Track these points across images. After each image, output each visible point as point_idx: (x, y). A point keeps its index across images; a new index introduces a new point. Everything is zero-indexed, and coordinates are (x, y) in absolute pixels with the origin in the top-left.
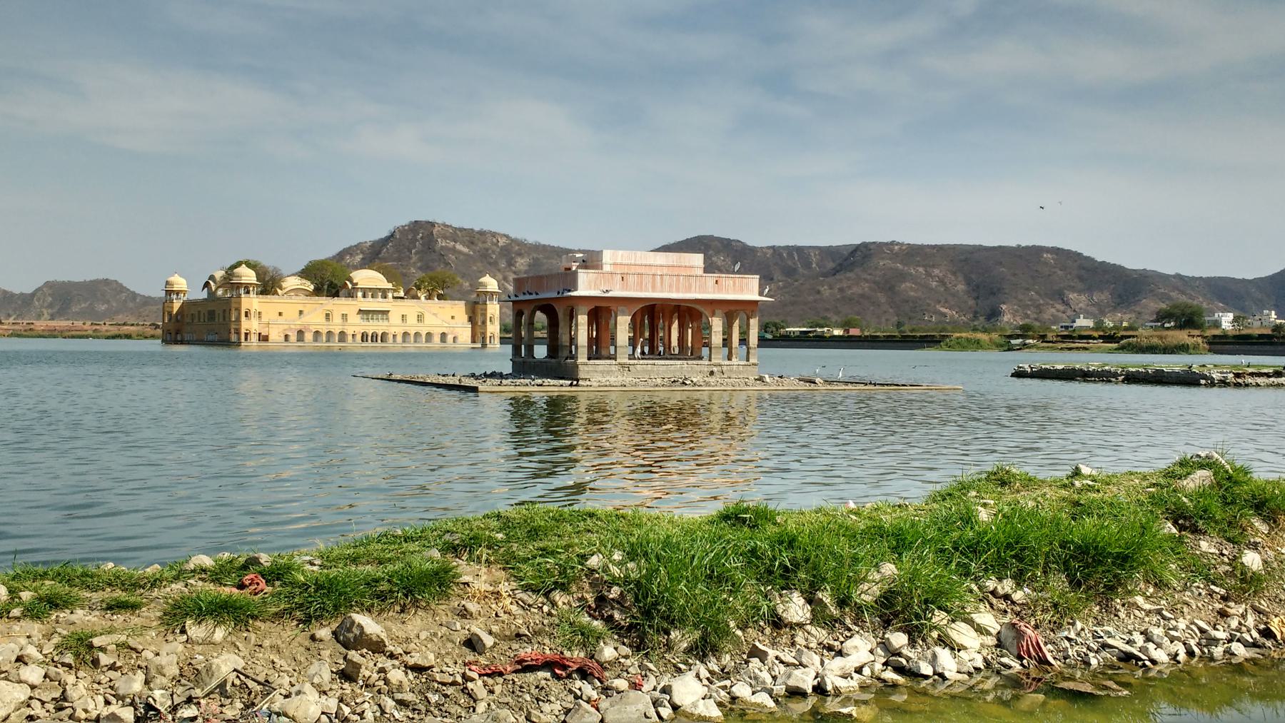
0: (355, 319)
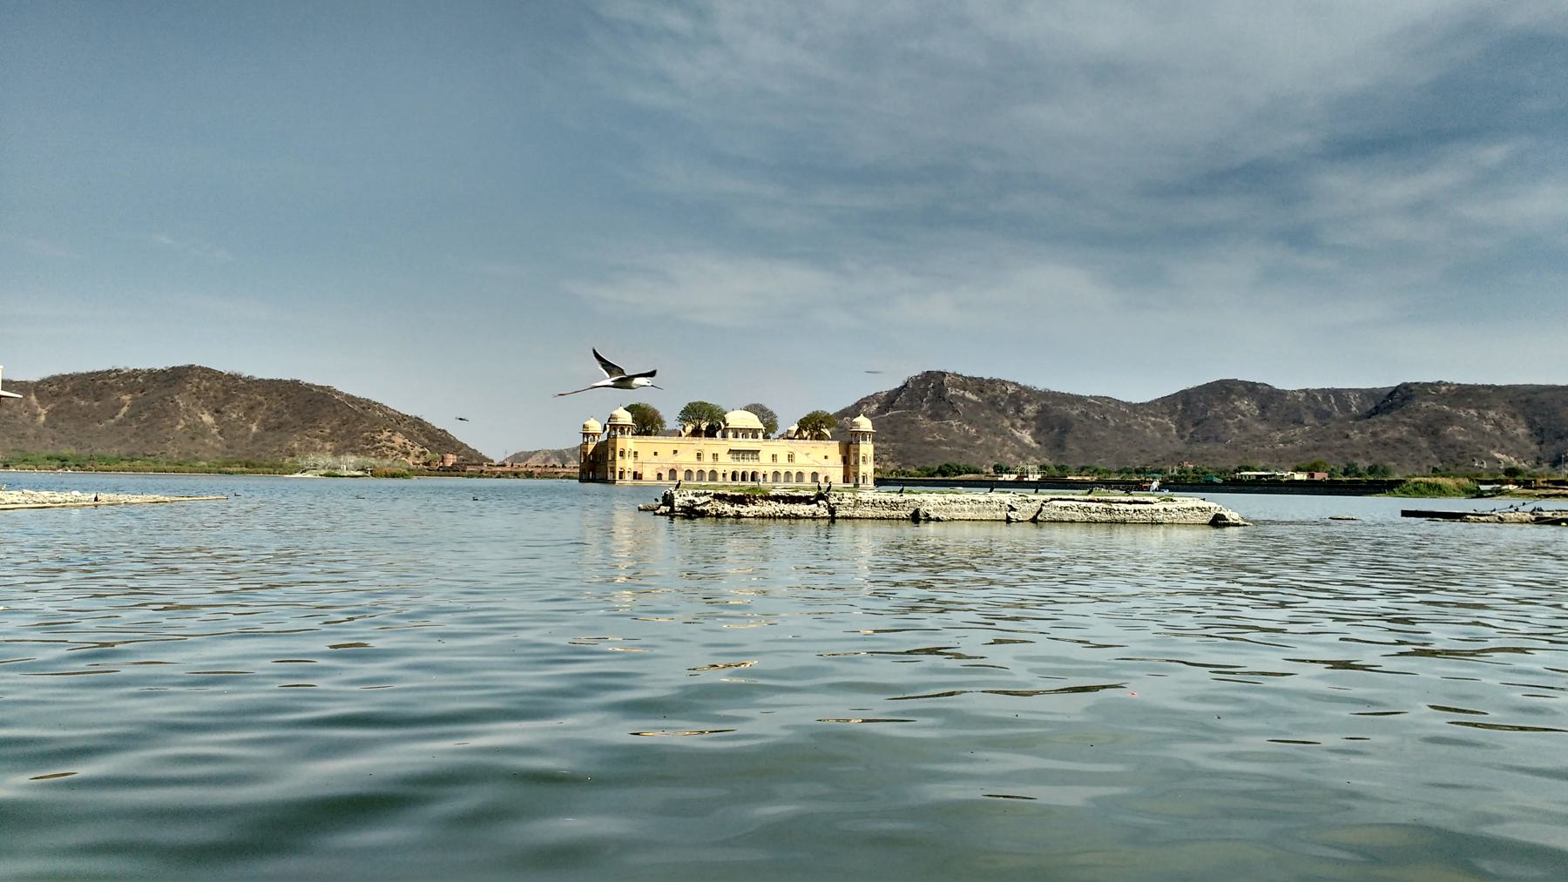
0: (725, 458)
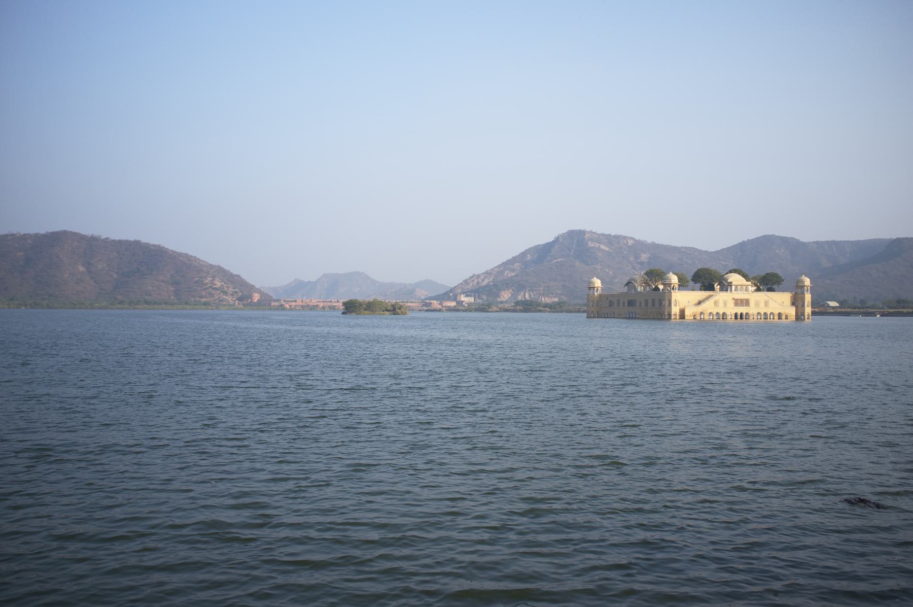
0: (731, 304)
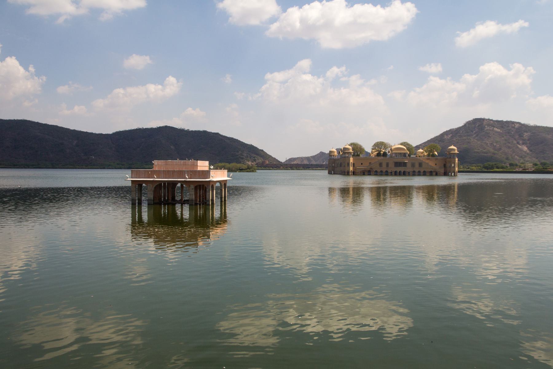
0: (391, 165)
